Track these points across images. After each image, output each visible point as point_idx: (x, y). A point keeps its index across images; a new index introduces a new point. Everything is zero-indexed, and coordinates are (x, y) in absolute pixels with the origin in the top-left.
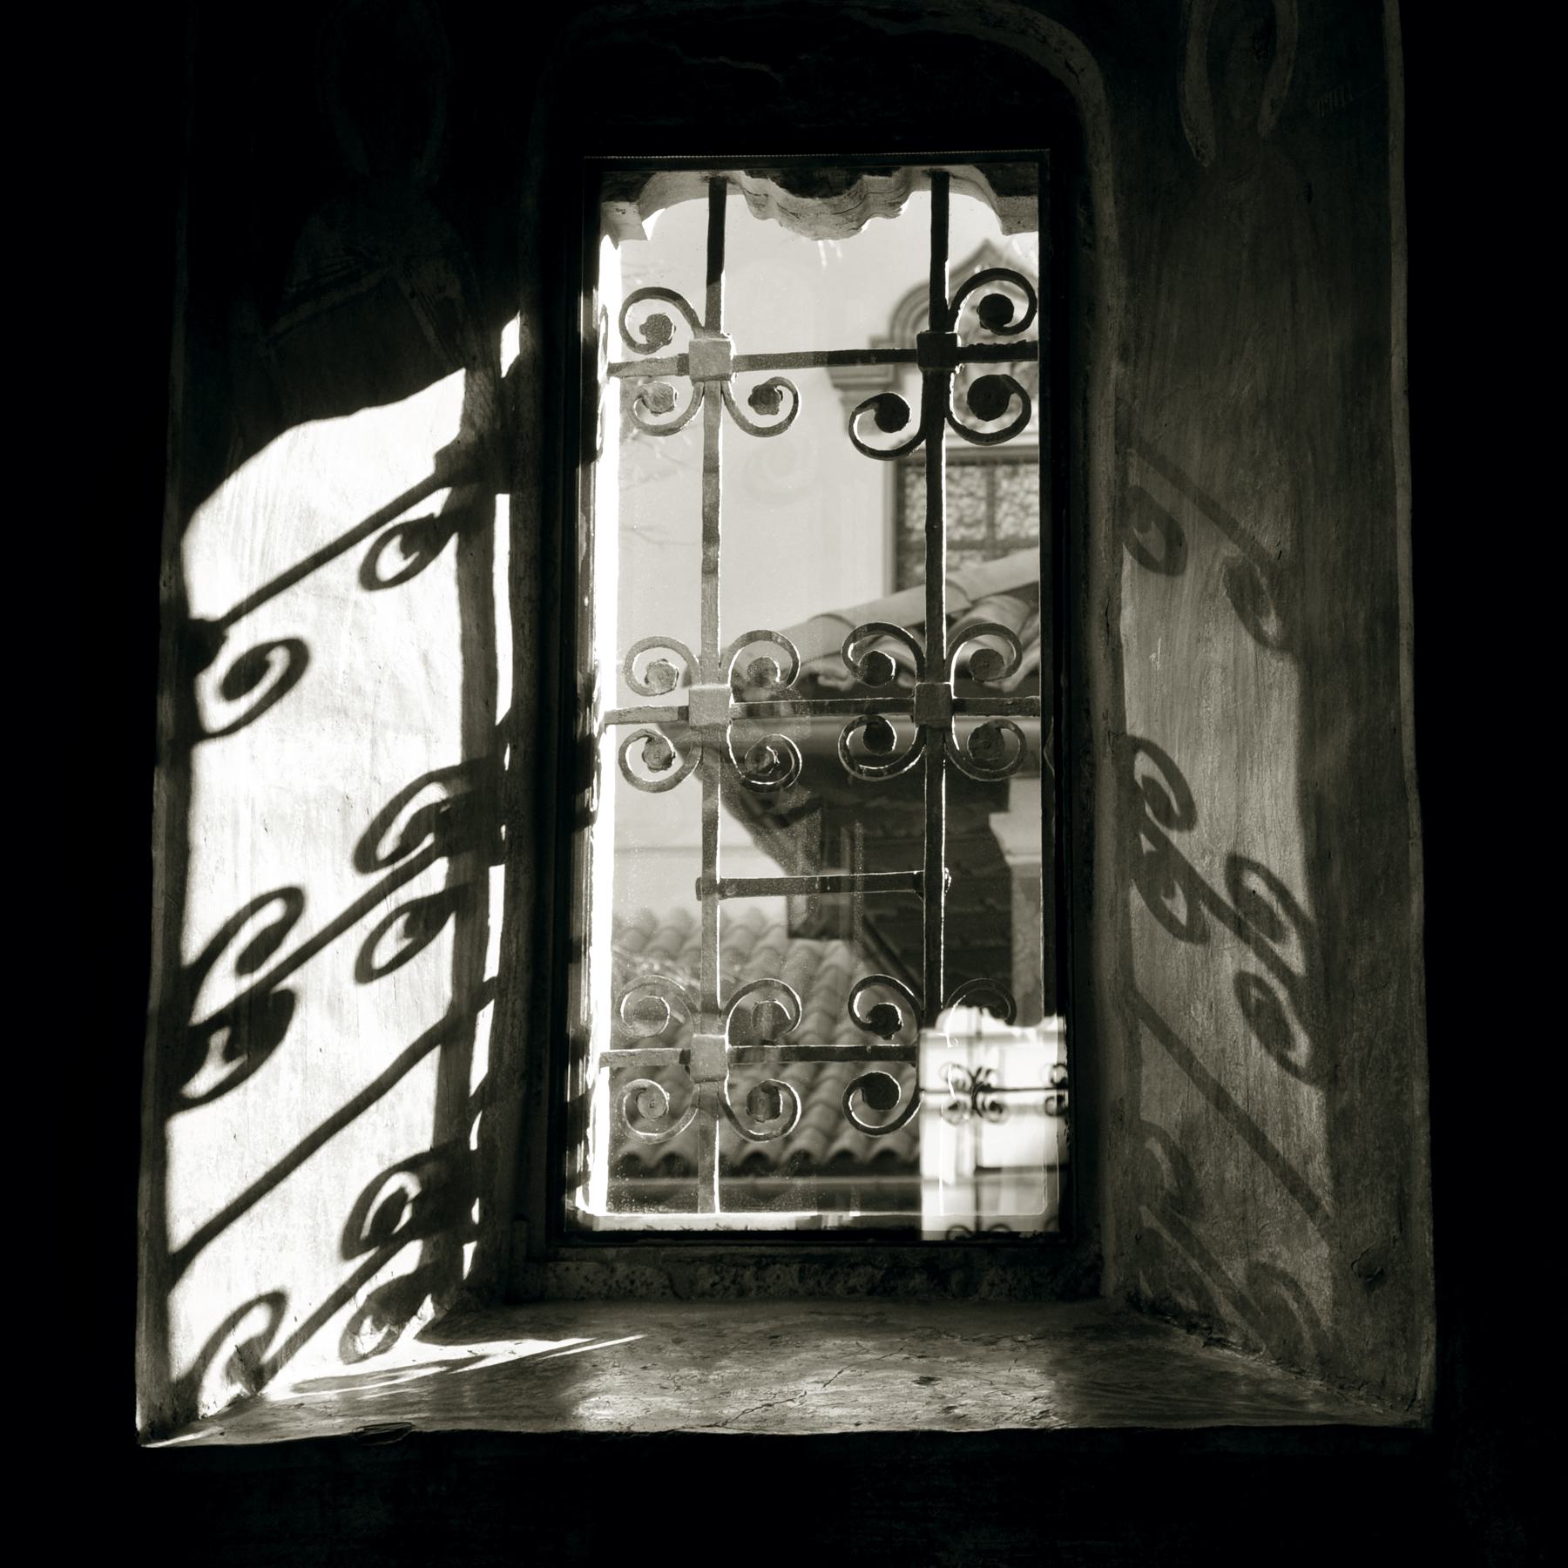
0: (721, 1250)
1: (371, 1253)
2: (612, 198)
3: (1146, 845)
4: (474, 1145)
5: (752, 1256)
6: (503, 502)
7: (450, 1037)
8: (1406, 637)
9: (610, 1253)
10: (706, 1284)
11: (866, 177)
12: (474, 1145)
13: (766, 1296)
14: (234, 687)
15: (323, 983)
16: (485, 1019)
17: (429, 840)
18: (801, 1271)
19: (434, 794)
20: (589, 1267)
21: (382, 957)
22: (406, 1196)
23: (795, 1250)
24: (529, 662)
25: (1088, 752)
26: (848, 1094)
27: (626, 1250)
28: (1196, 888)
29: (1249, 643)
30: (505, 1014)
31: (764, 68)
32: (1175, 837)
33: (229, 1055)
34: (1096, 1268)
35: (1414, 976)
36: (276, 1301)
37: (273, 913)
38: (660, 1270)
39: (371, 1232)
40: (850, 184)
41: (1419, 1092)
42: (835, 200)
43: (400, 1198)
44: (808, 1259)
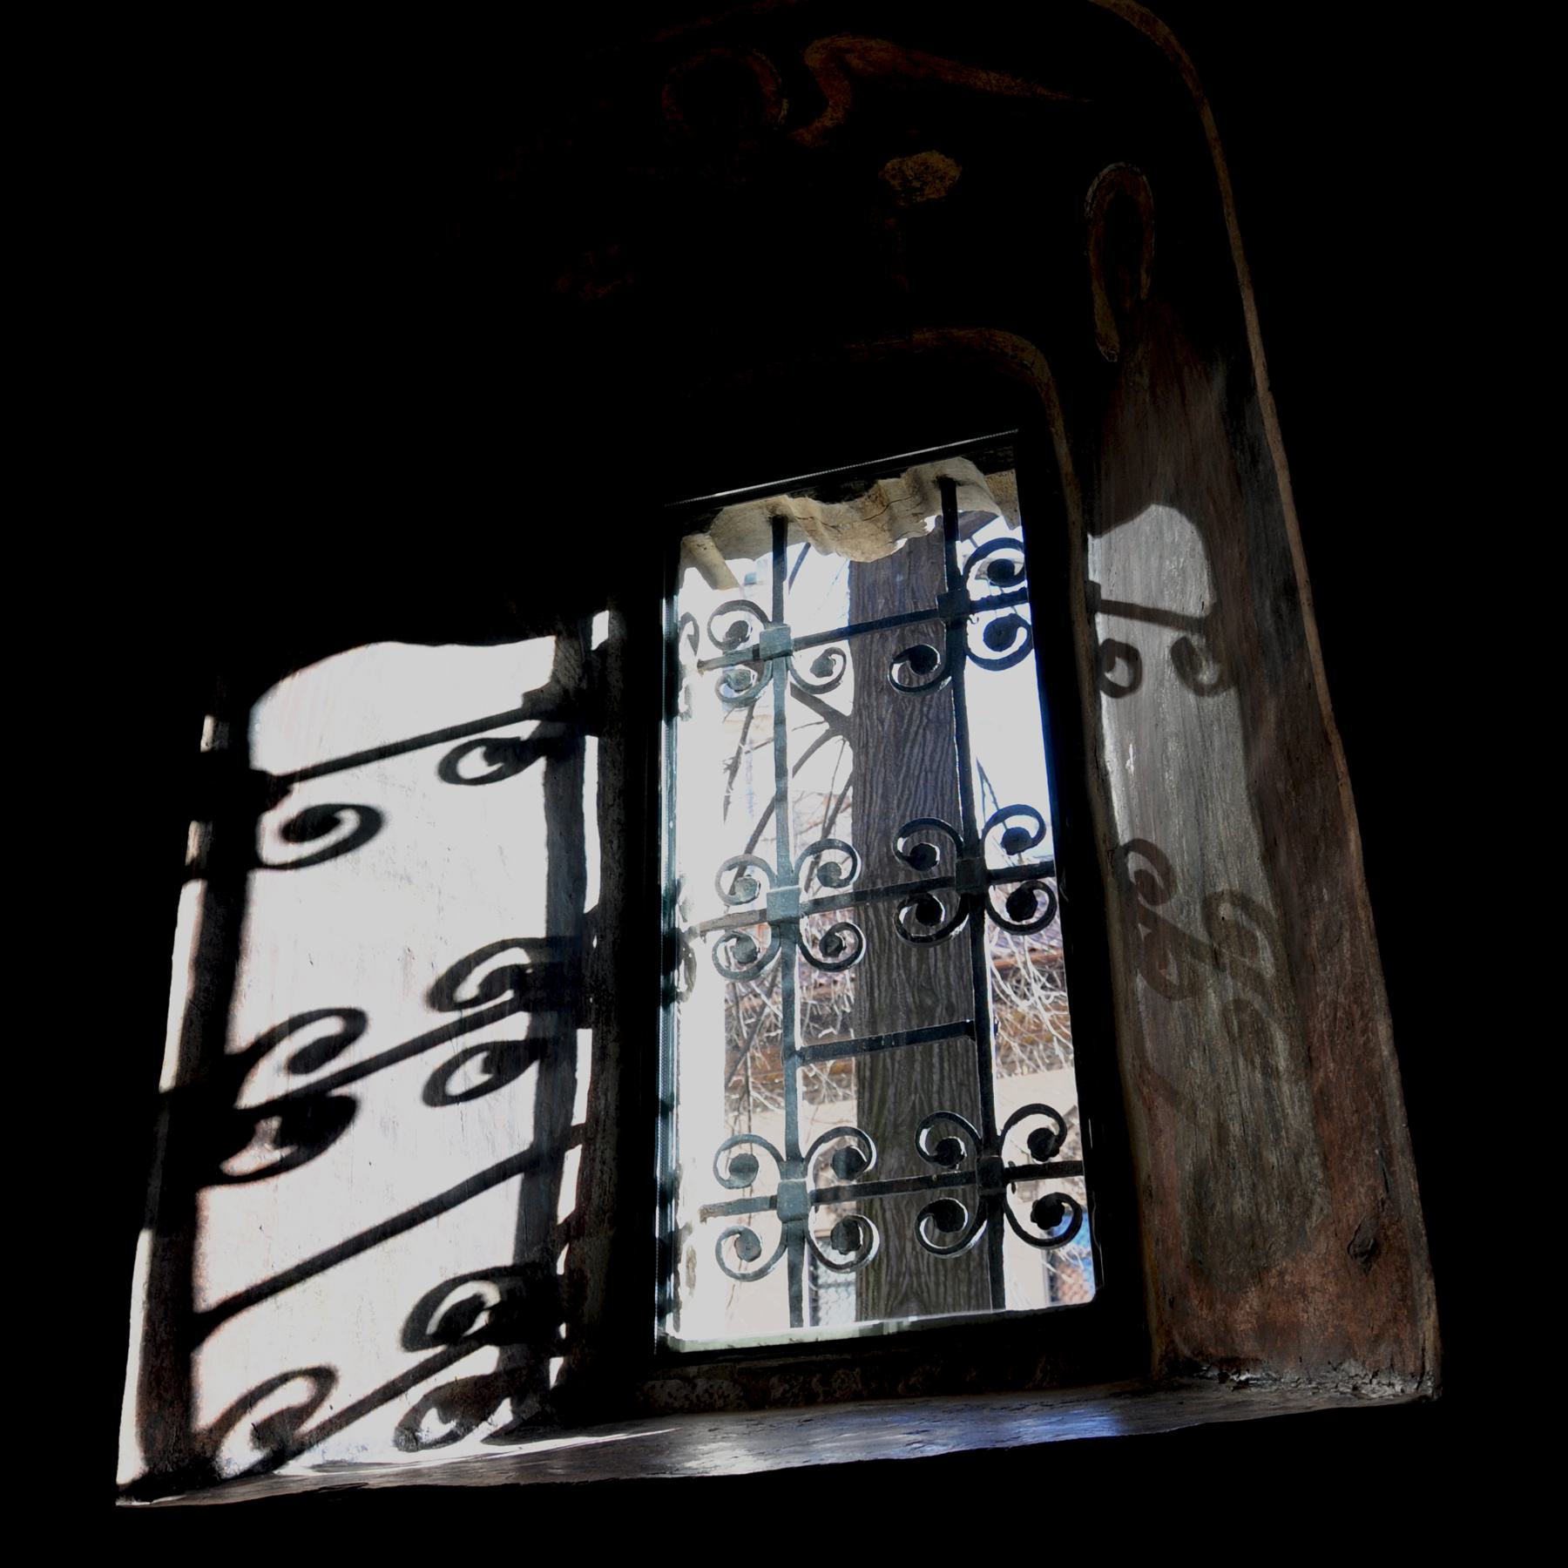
1: (439, 1349)
3: (1143, 931)
4: (560, 1270)
7: (536, 1167)
9: (692, 1370)
10: (777, 1393)
12: (560, 1270)
13: (830, 1399)
14: (294, 832)
15: (386, 1099)
16: (573, 1159)
17: (508, 995)
19: (518, 957)
20: (673, 1384)
21: (456, 1085)
24: (617, 871)
26: (920, 1220)
27: (705, 1367)
29: (1191, 697)
30: (593, 1160)
32: (1160, 910)
33: (280, 1141)
36: (323, 1377)
37: (332, 1027)
38: (735, 1382)
39: (439, 1328)
43: (476, 1304)
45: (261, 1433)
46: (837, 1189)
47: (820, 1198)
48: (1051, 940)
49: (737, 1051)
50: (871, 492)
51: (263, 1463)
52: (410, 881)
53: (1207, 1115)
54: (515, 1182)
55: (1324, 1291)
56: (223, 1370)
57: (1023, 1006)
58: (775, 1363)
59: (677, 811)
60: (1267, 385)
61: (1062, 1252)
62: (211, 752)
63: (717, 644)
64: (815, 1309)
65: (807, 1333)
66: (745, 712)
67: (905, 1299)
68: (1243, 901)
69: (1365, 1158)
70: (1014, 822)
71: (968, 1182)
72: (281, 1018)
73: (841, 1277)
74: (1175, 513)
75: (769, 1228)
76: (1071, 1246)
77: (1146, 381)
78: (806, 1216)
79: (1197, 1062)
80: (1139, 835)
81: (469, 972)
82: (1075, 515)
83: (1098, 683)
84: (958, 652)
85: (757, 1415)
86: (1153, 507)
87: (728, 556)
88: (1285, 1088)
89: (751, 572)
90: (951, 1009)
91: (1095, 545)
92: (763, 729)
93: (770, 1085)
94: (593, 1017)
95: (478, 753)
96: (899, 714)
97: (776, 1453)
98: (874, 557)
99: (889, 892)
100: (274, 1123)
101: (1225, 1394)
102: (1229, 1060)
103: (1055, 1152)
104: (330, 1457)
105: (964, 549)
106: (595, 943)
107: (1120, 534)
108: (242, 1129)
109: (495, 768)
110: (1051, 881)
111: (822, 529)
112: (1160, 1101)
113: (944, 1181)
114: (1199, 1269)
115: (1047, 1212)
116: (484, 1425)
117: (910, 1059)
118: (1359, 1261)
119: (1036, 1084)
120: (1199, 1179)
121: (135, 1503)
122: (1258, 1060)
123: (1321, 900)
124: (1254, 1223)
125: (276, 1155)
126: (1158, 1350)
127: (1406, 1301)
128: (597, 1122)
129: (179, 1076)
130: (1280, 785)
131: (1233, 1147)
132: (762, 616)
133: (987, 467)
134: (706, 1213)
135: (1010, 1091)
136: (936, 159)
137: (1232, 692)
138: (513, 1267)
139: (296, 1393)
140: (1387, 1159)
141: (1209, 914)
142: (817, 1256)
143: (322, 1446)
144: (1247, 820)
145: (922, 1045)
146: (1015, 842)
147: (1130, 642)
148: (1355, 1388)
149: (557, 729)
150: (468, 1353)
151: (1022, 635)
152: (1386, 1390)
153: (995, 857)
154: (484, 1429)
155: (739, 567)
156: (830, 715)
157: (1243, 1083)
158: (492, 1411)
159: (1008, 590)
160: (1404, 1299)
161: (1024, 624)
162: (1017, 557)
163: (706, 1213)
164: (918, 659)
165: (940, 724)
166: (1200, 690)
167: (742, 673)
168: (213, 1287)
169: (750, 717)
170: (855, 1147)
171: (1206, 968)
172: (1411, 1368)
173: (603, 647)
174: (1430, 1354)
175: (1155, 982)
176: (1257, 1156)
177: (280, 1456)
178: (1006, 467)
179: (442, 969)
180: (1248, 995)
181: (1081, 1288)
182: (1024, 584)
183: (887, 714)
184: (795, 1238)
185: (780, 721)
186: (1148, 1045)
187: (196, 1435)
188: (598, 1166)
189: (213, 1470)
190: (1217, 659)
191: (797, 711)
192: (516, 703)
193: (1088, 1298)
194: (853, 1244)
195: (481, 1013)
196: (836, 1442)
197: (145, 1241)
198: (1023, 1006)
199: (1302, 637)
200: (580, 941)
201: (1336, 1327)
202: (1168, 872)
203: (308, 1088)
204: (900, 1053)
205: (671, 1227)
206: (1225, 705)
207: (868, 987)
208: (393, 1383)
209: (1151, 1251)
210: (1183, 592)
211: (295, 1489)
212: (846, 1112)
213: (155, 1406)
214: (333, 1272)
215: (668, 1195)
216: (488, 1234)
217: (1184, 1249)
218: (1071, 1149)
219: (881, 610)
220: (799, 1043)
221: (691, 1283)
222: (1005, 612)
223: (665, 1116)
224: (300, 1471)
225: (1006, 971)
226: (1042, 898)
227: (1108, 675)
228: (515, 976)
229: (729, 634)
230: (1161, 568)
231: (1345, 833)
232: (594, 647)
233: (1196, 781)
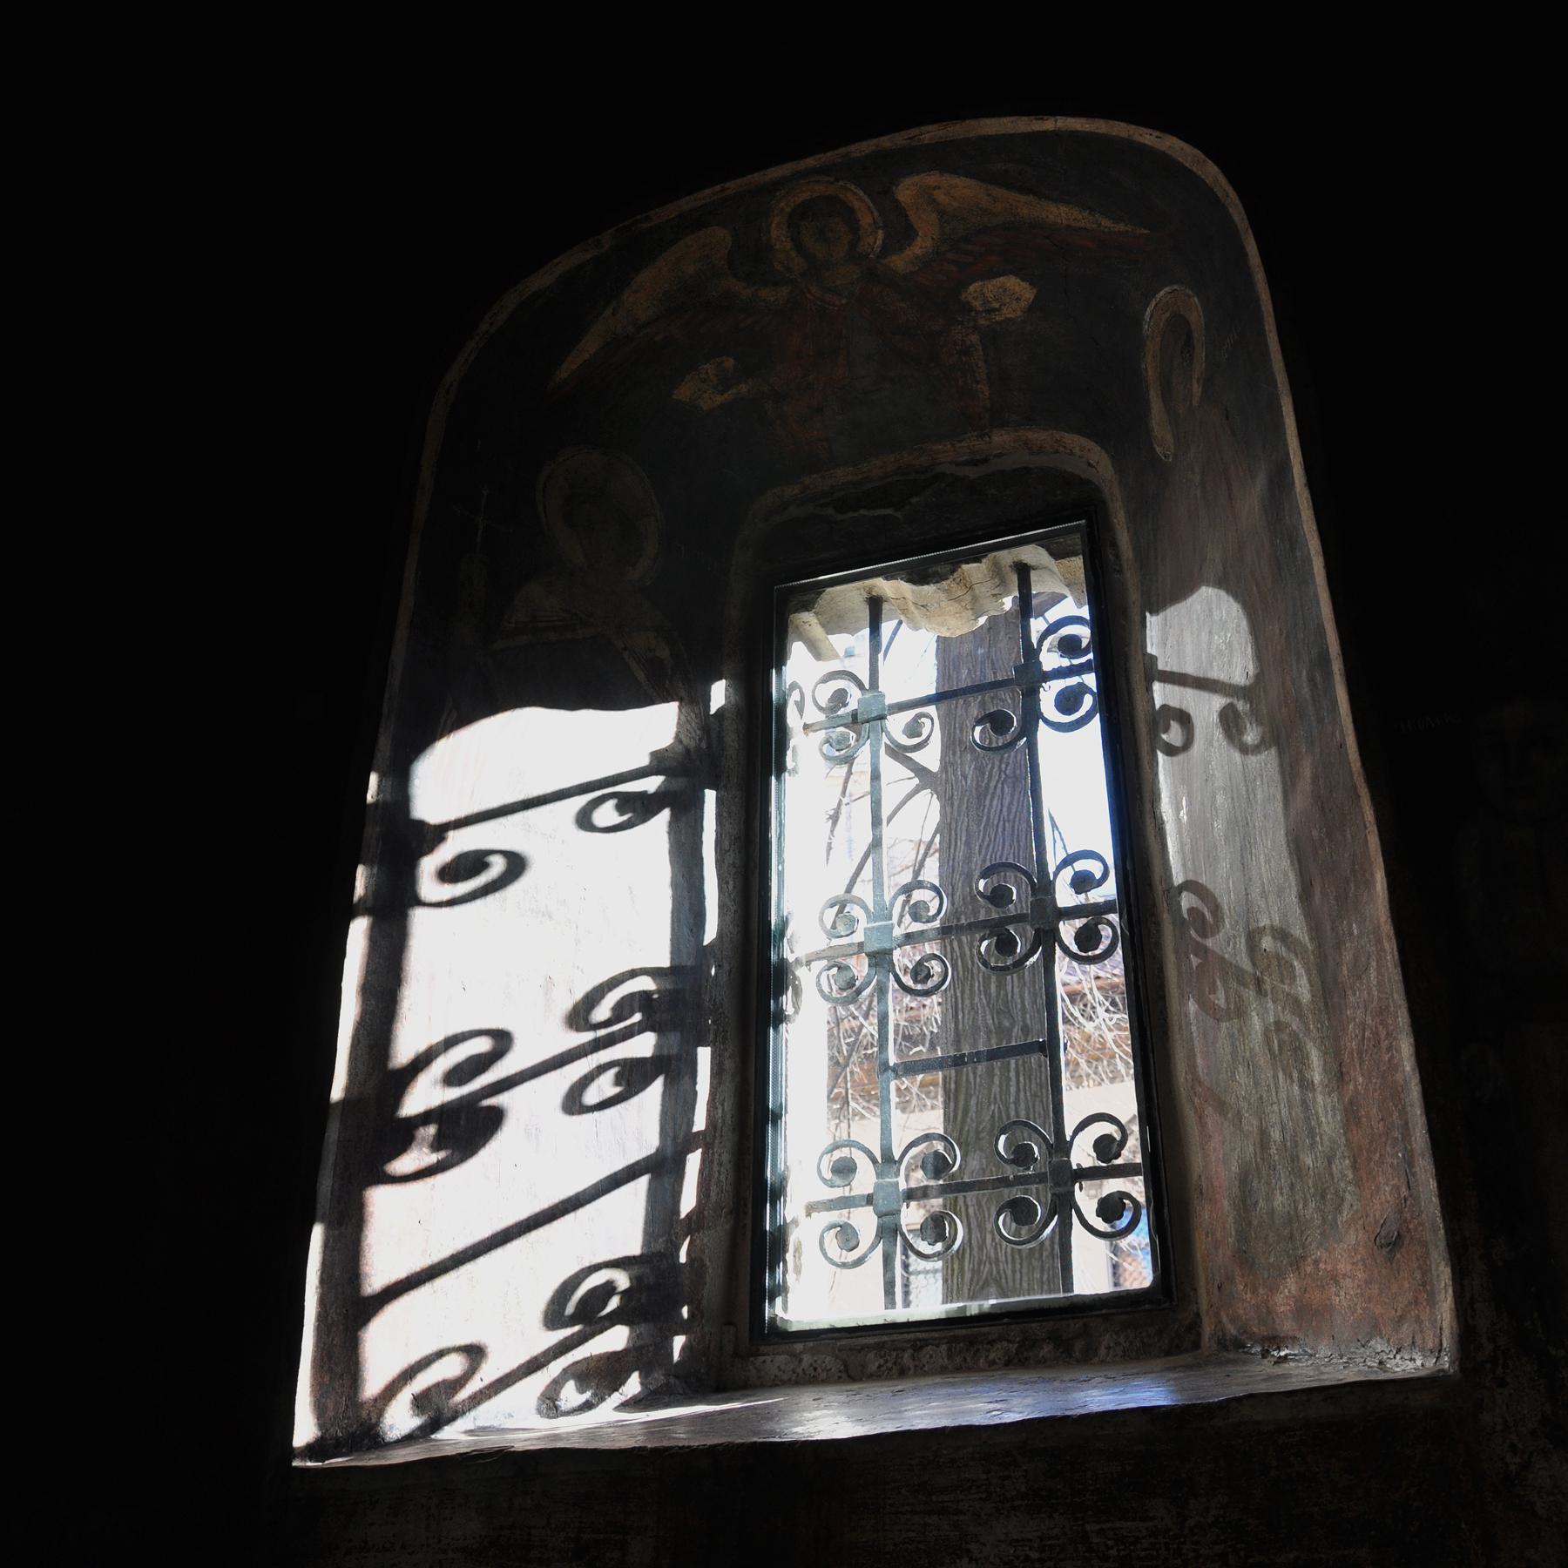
0: (885, 1338)
2: (797, 611)
3: (1195, 961)
4: (683, 1259)
5: (908, 1341)
6: (710, 796)
7: (661, 1168)
8: (1337, 666)
9: (799, 1347)
10: (873, 1367)
11: (965, 567)
12: (683, 1259)
13: (920, 1371)
14: (448, 874)
15: (531, 1109)
16: (694, 1161)
17: (637, 1017)
18: (949, 1350)
19: (646, 984)
20: (781, 1359)
23: (943, 1334)
25: (1153, 915)
26: (998, 1215)
28: (1228, 969)
29: (1237, 756)
30: (712, 1162)
31: (889, 511)
32: (1209, 943)
33: (436, 1146)
34: (1195, 1326)
35: (1387, 945)
36: (475, 1353)
37: (483, 1045)
38: (837, 1357)
39: (575, 1310)
40: (953, 572)
41: (1406, 1047)
43: (608, 1289)
44: (955, 1339)
45: (420, 1402)
46: (926, 1187)
47: (910, 1195)
48: (1114, 969)
49: (838, 1066)
51: (421, 1428)
53: (1250, 1123)
55: (1353, 1278)
56: (386, 1347)
57: (1089, 1027)
58: (871, 1341)
59: (786, 856)
60: (1304, 481)
61: (1123, 1243)
62: (376, 805)
63: (821, 709)
64: (906, 1293)
65: (900, 1314)
66: (845, 768)
67: (986, 1284)
68: (1282, 935)
69: (1390, 1160)
70: (1081, 865)
71: (1040, 1182)
72: (437, 1037)
73: (929, 1265)
74: (1223, 593)
75: (865, 1222)
76: (1131, 1238)
77: (1197, 478)
79: (1242, 1076)
80: (1191, 877)
81: (603, 997)
82: (1134, 596)
83: (1155, 743)
84: (1032, 716)
85: (856, 1386)
86: (1204, 588)
87: (830, 632)
88: (1320, 1099)
89: (851, 646)
90: (1026, 1030)
91: (1153, 621)
92: (861, 783)
93: (868, 1097)
94: (712, 1036)
95: (611, 803)
96: (980, 770)
97: (872, 1420)
98: (958, 633)
99: (972, 927)
100: (432, 1130)
101: (1267, 1367)
102: (1270, 1074)
103: (1118, 1155)
104: (480, 1423)
105: (1037, 626)
107: (1175, 612)
108: (402, 1135)
109: (625, 817)
110: (1114, 918)
111: (912, 608)
112: (1209, 1110)
113: (1020, 1181)
114: (1244, 1258)
115: (1110, 1208)
116: (616, 1394)
117: (990, 1073)
118: (1385, 1251)
119: (1100, 1096)
120: (1244, 1179)
121: (309, 1464)
122: (1295, 1075)
123: (1351, 934)
124: (1292, 1218)
125: (433, 1158)
126: (1207, 1329)
127: (1426, 1286)
128: (715, 1128)
129: (348, 1089)
130: (1315, 833)
131: (1273, 1150)
132: (860, 685)
133: (1057, 555)
134: (811, 1209)
135: (1077, 1103)
136: (1013, 283)
137: (1273, 751)
138: (641, 1256)
139: (452, 1367)
140: (1409, 1161)
142: (908, 1246)
143: (473, 1413)
144: (1286, 863)
145: (1001, 1061)
146: (1082, 883)
148: (1381, 1363)
149: (679, 783)
150: (601, 1332)
151: (1088, 701)
152: (1408, 1365)
153: (1065, 896)
154: (616, 1399)
155: (839, 641)
156: (920, 771)
157: (1283, 1095)
158: (623, 1383)
159: (1076, 662)
160: (1424, 1284)
161: (1089, 691)
162: (1084, 633)
163: (811, 1209)
164: (997, 722)
165: (1016, 779)
166: (1244, 750)
167: (842, 734)
168: (378, 1272)
169: (849, 773)
170: (941, 1150)
171: (1250, 994)
172: (1430, 1345)
173: (720, 711)
174: (1446, 1332)
175: (1206, 1006)
176: (1295, 1159)
177: (435, 1424)
179: (579, 995)
181: (1140, 1275)
182: (1091, 656)
183: (970, 771)
184: (889, 1231)
185: (876, 776)
186: (1199, 1061)
187: (362, 1404)
188: (716, 1168)
189: (377, 1435)
190: (1259, 722)
191: (892, 770)
192: (644, 761)
193: (1147, 1283)
194: (939, 1236)
196: (925, 1410)
197: (317, 1234)
198: (1089, 1027)
199: (1335, 703)
200: (699, 970)
201: (1364, 1309)
202: (1216, 909)
203: (462, 1098)
204: (981, 1068)
205: (780, 1221)
206: (1267, 762)
207: (953, 1009)
208: (536, 1358)
209: (1201, 1244)
210: (1230, 663)
211: (449, 1451)
212: (933, 1119)
213: (327, 1378)
214: (483, 1261)
215: (778, 1192)
216: (620, 1226)
218: (1132, 1152)
219: (964, 679)
220: (893, 1060)
221: (798, 1271)
222: (1073, 681)
223: (775, 1124)
224: (455, 1436)
225: (1074, 996)
226: (1106, 932)
227: (1164, 736)
228: (642, 1001)
229: (831, 700)
230: (1210, 643)
231: (1372, 875)
232: (713, 711)
233: (1241, 828)
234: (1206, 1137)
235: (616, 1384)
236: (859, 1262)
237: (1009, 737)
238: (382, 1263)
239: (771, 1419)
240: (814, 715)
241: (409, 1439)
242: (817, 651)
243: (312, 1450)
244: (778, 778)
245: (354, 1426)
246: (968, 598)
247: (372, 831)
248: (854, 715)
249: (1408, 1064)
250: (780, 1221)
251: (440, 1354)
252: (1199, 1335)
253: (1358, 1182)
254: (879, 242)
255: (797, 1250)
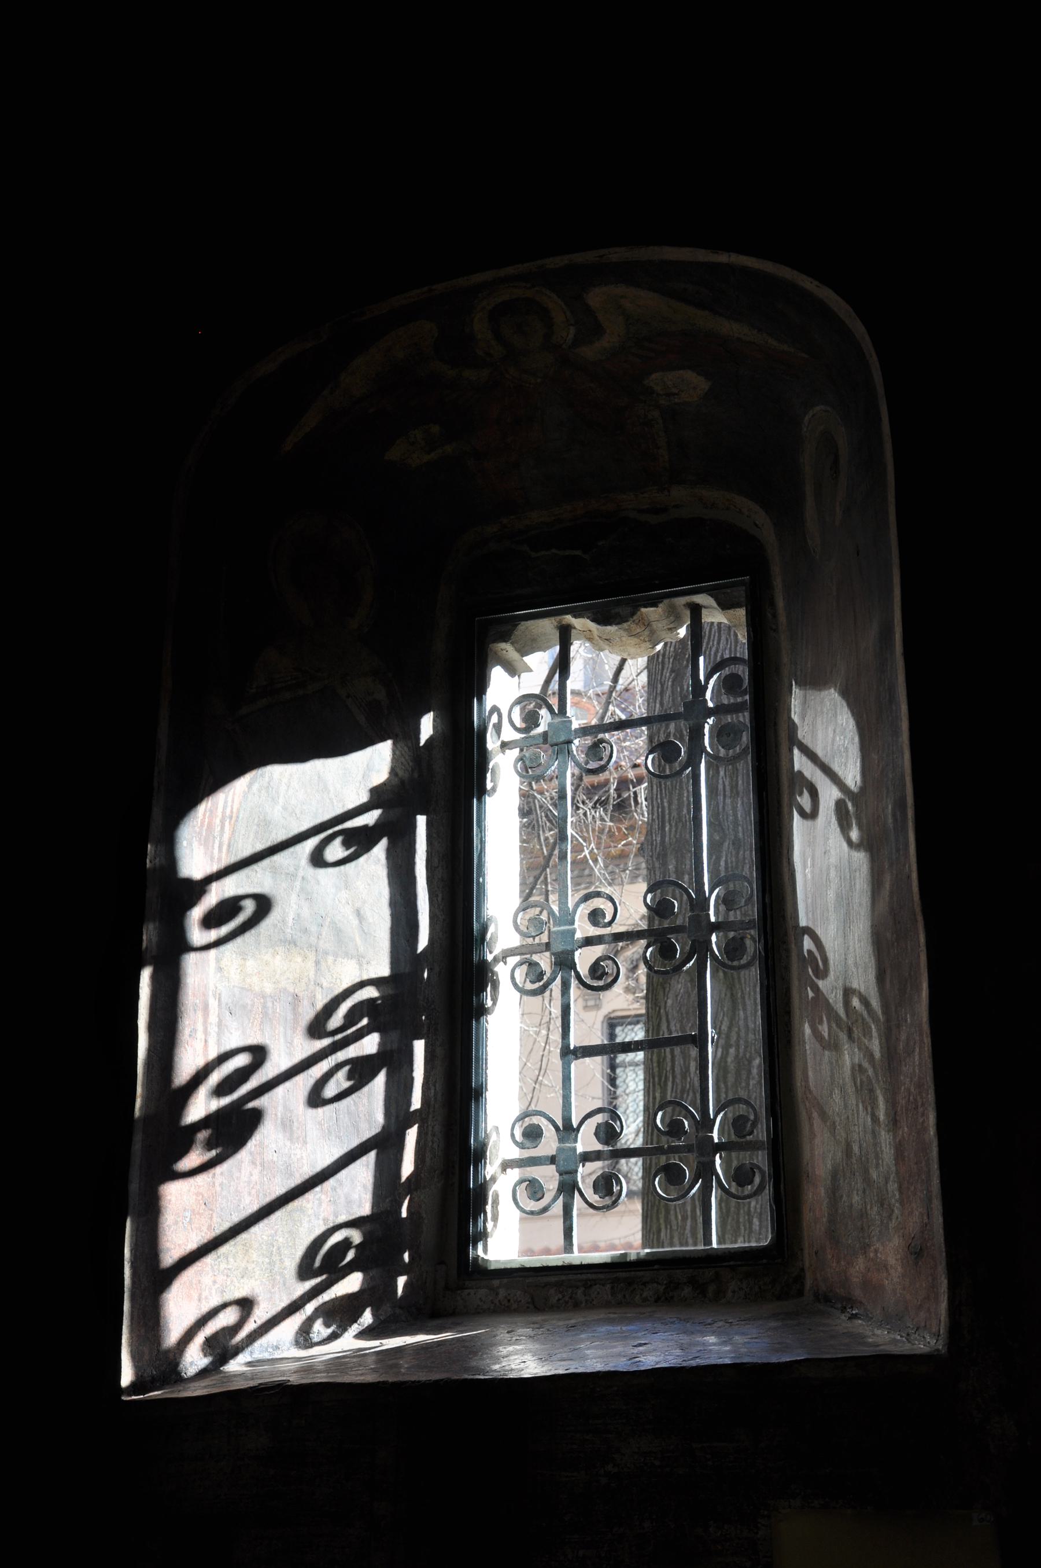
1: (324, 1277)
4: (404, 1214)
7: (385, 1145)
11: (643, 610)
12: (404, 1214)
16: (412, 1135)
21: (330, 1090)
22: (351, 1243)
30: (426, 1134)
40: (633, 614)
42: (625, 625)
50: (635, 617)
52: (296, 945)
54: (373, 1154)
65: (576, 1257)
68: (865, 1002)
71: (689, 1151)
75: (549, 1177)
78: (576, 1171)
80: (811, 925)
85: (539, 1318)
88: (883, 1133)
94: (425, 1030)
102: (854, 1102)
103: (751, 1133)
106: (426, 975)
109: (352, 850)
113: (673, 1150)
120: (835, 1175)
122: (869, 1109)
123: (906, 1021)
126: (809, 1283)
131: (854, 1161)
134: (506, 1165)
141: (847, 1003)
147: (813, 781)
154: (355, 1329)
157: (861, 1121)
163: (506, 1165)
171: (843, 1036)
175: (817, 1034)
176: (866, 1171)
178: (737, 605)
179: (320, 1005)
180: (866, 1064)
184: (568, 1187)
186: (810, 1074)
188: (430, 1138)
192: (364, 798)
195: (347, 1036)
199: (906, 838)
205: (480, 1180)
209: (807, 1216)
213: (143, 1331)
215: (480, 1156)
216: (355, 1192)
217: (825, 1220)
218: (761, 1133)
221: (495, 1218)
223: (477, 1100)
230: (834, 740)
234: (813, 1135)
235: (354, 1317)
236: (545, 1210)
237: (677, 766)
238: (177, 1239)
239: (475, 1353)
240: (509, 734)
241: (203, 1373)
242: (512, 670)
243: (134, 1388)
244: (480, 800)
245: (162, 1366)
246: (647, 633)
247: (152, 894)
248: (545, 734)
249: (932, 1131)
250: (480, 1180)
251: (224, 1306)
252: (803, 1285)
253: (901, 1202)
254: (571, 336)
255: (496, 1202)
